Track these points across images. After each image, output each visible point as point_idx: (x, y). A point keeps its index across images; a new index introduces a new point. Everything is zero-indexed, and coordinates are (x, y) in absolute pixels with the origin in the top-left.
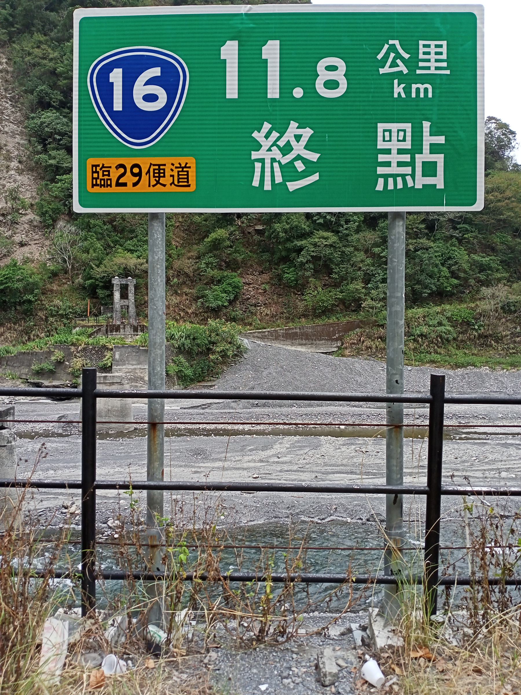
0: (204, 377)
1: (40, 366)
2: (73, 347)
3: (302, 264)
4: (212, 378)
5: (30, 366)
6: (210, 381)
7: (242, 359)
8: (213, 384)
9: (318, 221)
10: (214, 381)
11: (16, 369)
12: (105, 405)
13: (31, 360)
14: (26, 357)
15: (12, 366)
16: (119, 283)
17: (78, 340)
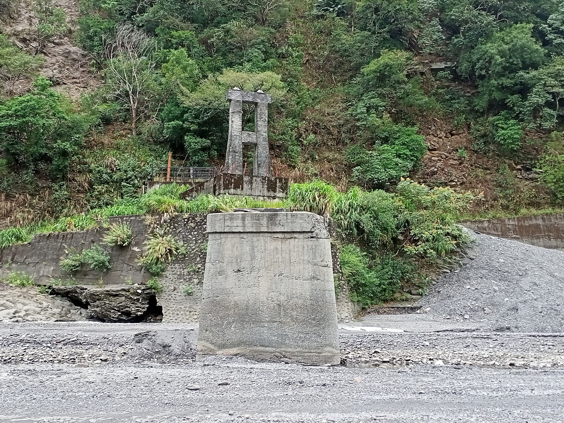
0: (394, 292)
1: (78, 257)
2: (149, 217)
3: (536, 110)
4: (409, 296)
5: (57, 260)
6: (407, 300)
7: (466, 260)
8: (415, 305)
9: (555, 41)
10: (415, 300)
11: (31, 269)
12: (270, 290)
13: (62, 248)
14: (52, 243)
15: (24, 263)
16: (240, 99)
17: (159, 202)
